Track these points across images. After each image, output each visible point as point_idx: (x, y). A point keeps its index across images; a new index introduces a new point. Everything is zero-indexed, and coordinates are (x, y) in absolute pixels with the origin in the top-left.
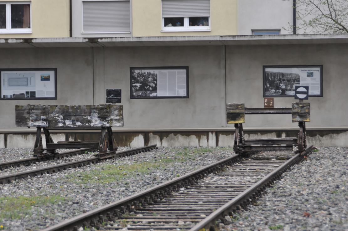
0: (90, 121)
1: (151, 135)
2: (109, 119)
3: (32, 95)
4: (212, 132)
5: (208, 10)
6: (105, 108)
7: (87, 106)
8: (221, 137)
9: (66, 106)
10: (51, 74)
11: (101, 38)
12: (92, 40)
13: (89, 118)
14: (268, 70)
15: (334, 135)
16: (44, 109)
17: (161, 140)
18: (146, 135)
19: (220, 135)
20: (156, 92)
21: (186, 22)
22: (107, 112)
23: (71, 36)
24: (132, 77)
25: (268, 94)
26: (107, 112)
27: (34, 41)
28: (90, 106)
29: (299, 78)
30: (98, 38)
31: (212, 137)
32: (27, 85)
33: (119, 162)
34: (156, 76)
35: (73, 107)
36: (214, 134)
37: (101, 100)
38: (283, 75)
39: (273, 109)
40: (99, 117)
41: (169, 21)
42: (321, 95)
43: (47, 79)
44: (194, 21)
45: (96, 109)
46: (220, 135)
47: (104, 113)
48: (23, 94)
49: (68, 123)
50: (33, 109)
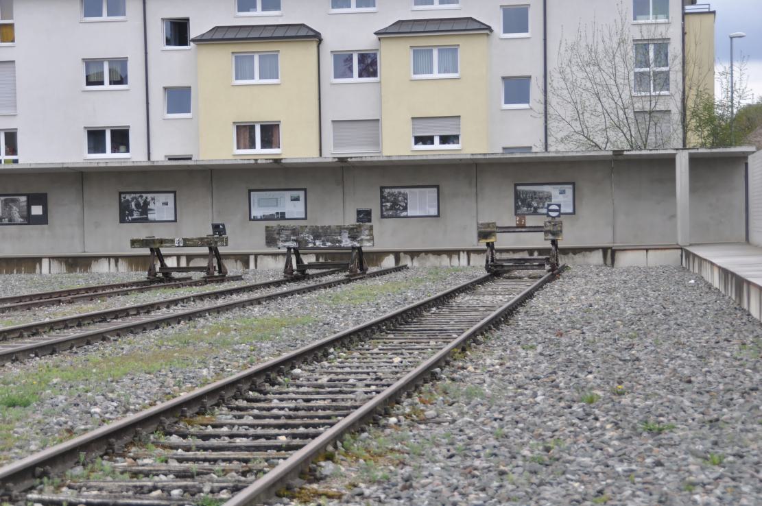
0: (340, 242)
1: (402, 254)
2: (359, 239)
3: (282, 216)
4: (463, 251)
5: (459, 127)
6: (356, 228)
7: (337, 226)
8: (473, 256)
9: (316, 226)
10: (301, 194)
11: (351, 158)
12: (342, 160)
13: (339, 238)
14: (519, 188)
15: (587, 253)
16: (294, 229)
17: (412, 259)
18: (397, 255)
19: (472, 254)
20: (407, 211)
21: (437, 140)
22: (358, 232)
23: (321, 155)
24: (382, 197)
25: (519, 212)
26: (358, 232)
27: (283, 161)
28: (340, 226)
29: (551, 196)
30: (347, 158)
31: (464, 256)
32: (277, 206)
33: (369, 282)
34: (407, 195)
35: (322, 227)
36: (465, 253)
38: (535, 193)
39: (526, 227)
40: (349, 237)
41: (419, 140)
42: (574, 213)
43: (297, 199)
44: (445, 140)
45: (346, 229)
46: (472, 254)
47: (354, 233)
48: (273, 215)
49: (318, 243)
50: (283, 229)
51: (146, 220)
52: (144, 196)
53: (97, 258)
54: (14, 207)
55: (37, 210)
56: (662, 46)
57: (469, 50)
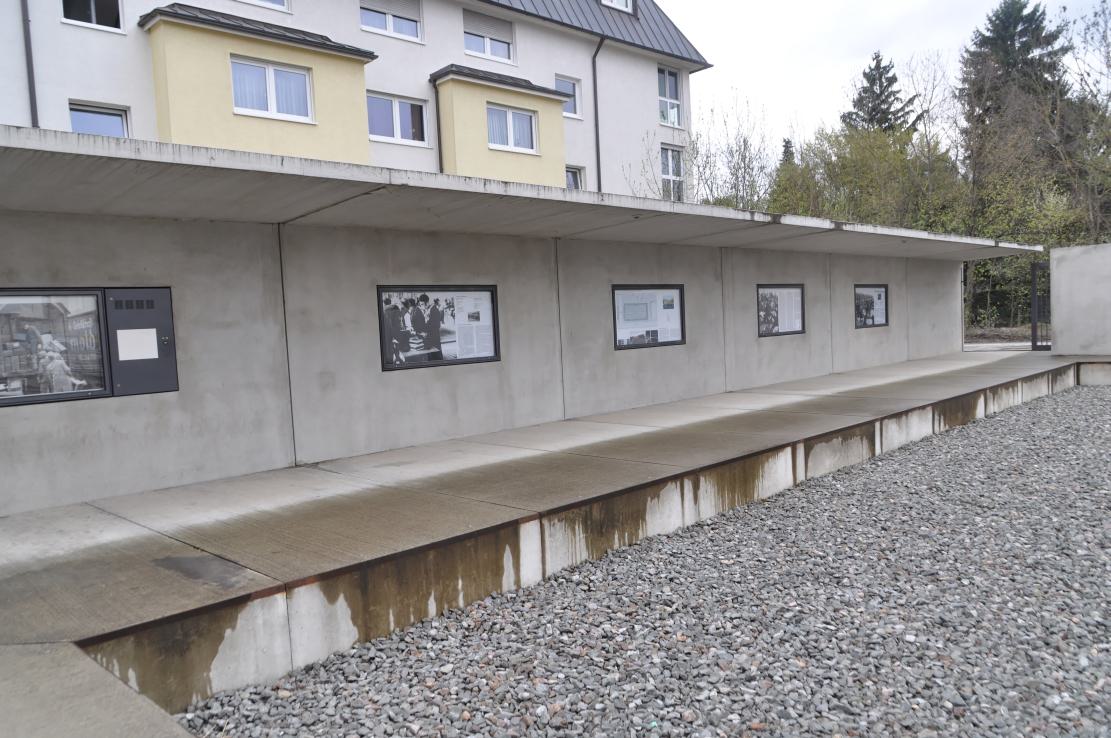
10: (674, 294)
32: (646, 318)
48: (641, 336)
51: (436, 360)
52: (432, 296)
53: (657, 485)
54: (46, 338)
55: (137, 344)
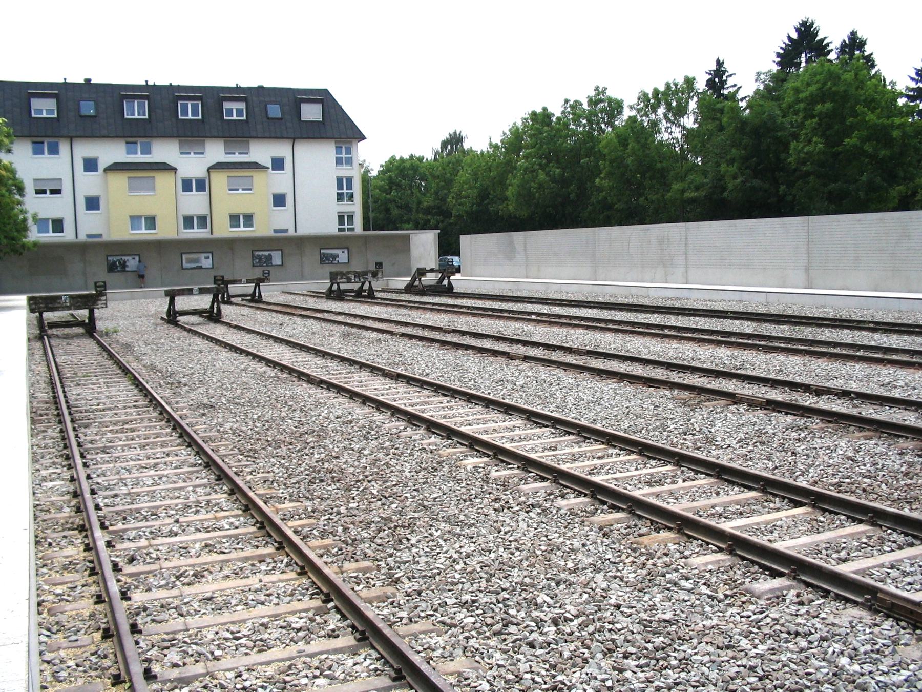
3: (201, 267)
10: (210, 255)
14: (322, 251)
37: (372, 267)
43: (209, 258)
51: (125, 271)
56: (349, 180)
57: (258, 178)
